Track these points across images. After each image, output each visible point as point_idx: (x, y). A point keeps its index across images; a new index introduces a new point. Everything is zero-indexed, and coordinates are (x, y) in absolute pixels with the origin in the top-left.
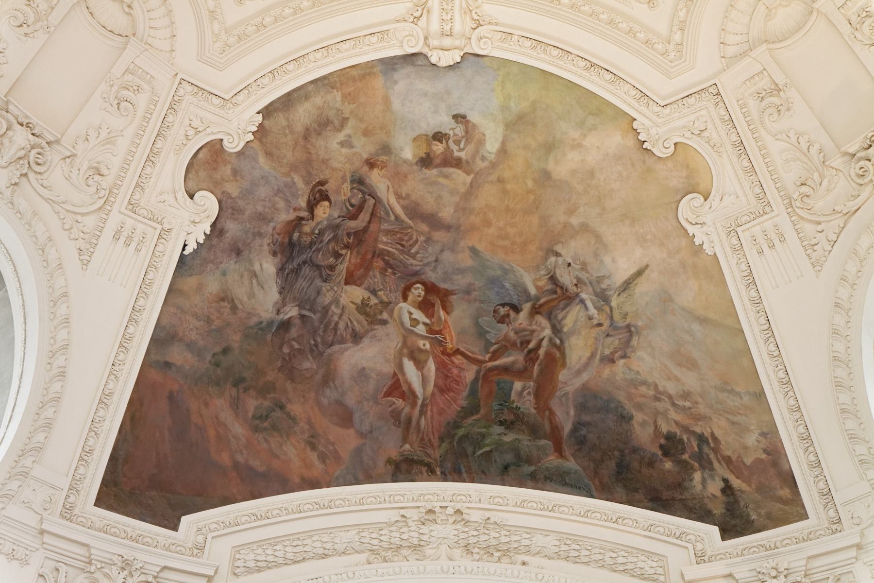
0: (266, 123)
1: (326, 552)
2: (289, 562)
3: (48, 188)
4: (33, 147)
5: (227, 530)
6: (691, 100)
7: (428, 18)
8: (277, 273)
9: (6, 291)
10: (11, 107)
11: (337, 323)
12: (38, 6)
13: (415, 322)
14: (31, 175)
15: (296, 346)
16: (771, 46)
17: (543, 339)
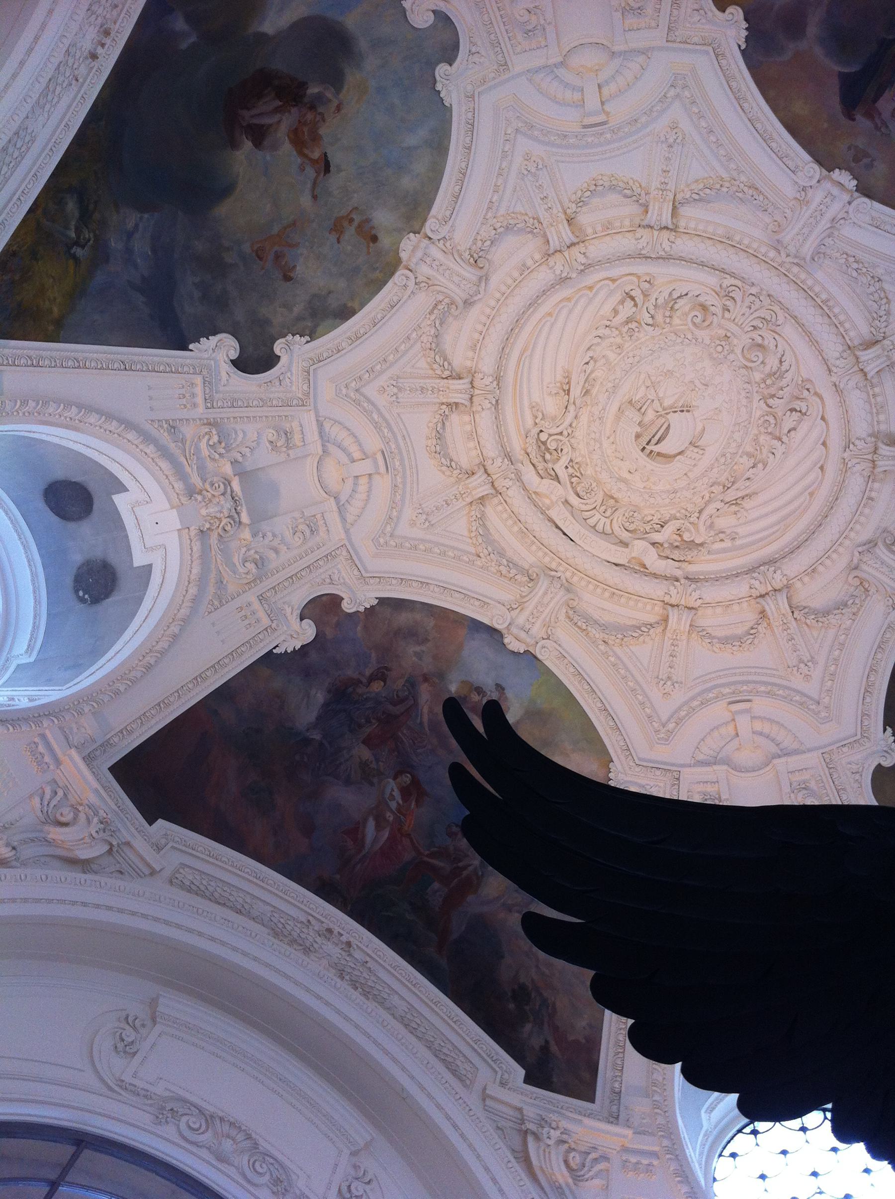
0: (378, 608)
1: (243, 910)
2: (212, 898)
5: (184, 848)
6: (658, 773)
7: (518, 614)
8: (323, 706)
9: (145, 594)
11: (341, 764)
13: (392, 797)
15: (306, 760)
16: (730, 770)
17: (470, 865)
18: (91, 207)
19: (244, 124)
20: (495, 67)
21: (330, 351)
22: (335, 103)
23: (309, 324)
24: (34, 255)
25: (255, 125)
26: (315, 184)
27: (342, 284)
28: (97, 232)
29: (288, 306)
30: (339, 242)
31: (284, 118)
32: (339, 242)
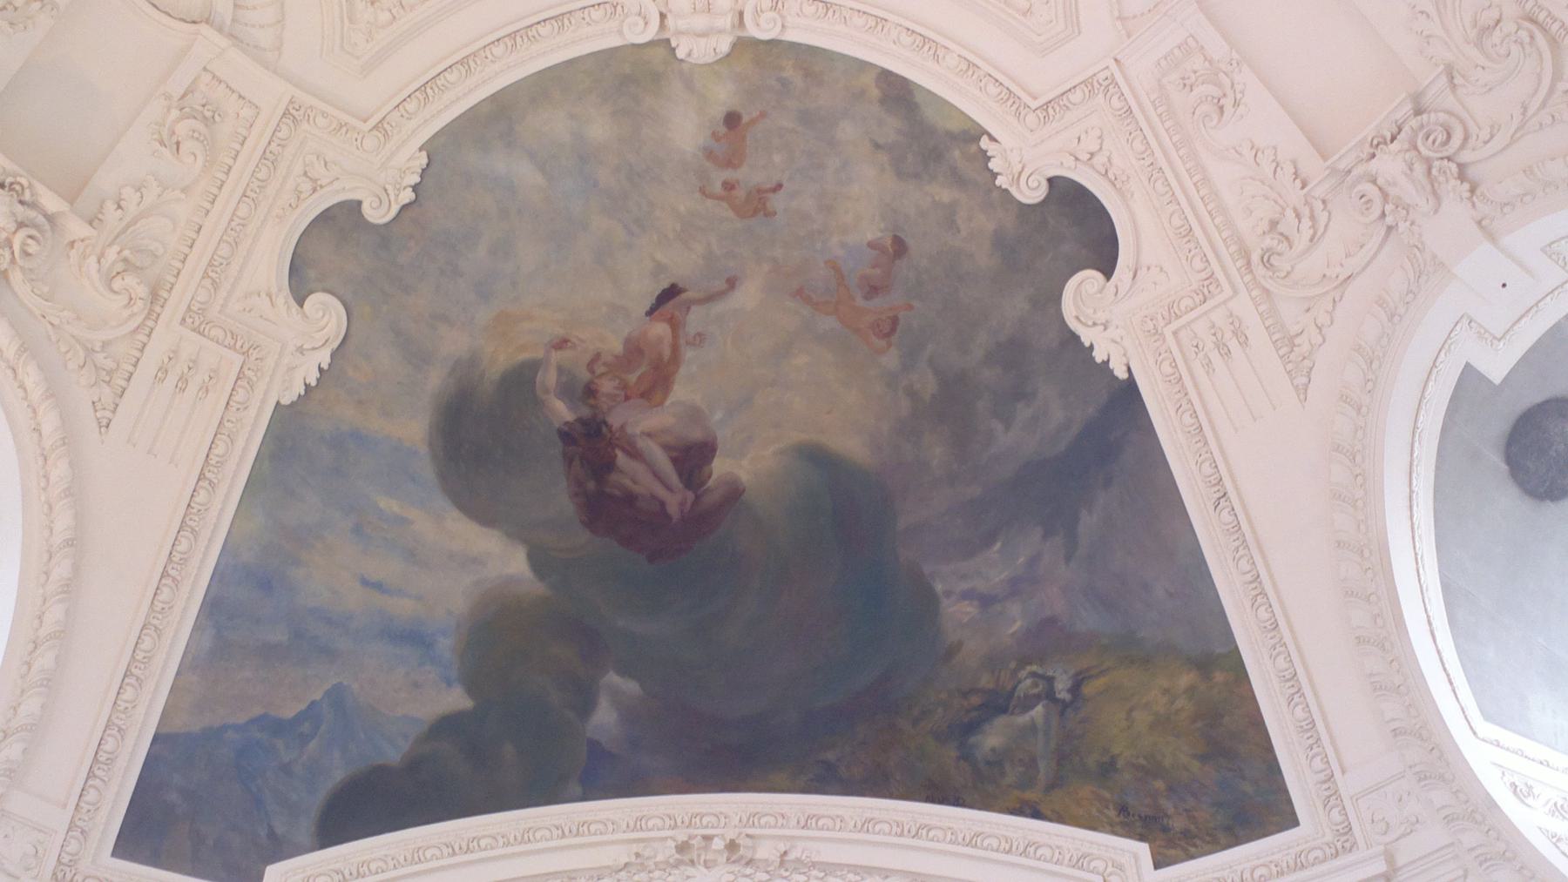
3: (1495, 131)
4: (1416, 148)
10: (1342, 166)
12: (1195, 72)
14: (1466, 156)
18: (975, 700)
19: (690, 496)
20: (305, 126)
21: (982, 84)
22: (556, 356)
23: (957, 153)
24: (1108, 769)
25: (680, 475)
26: (710, 298)
27: (847, 131)
28: (1013, 665)
29: (950, 223)
30: (779, 186)
31: (638, 431)
32: (779, 186)
